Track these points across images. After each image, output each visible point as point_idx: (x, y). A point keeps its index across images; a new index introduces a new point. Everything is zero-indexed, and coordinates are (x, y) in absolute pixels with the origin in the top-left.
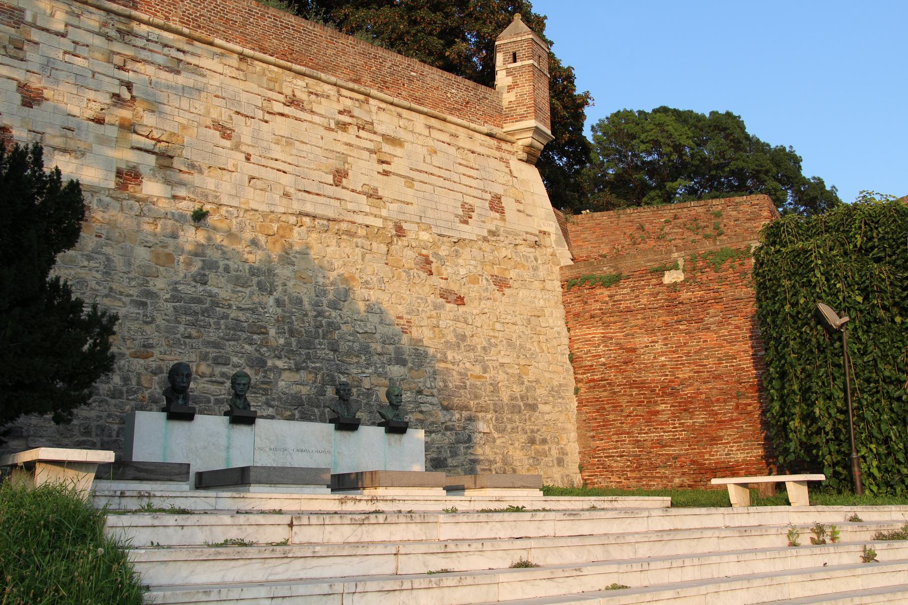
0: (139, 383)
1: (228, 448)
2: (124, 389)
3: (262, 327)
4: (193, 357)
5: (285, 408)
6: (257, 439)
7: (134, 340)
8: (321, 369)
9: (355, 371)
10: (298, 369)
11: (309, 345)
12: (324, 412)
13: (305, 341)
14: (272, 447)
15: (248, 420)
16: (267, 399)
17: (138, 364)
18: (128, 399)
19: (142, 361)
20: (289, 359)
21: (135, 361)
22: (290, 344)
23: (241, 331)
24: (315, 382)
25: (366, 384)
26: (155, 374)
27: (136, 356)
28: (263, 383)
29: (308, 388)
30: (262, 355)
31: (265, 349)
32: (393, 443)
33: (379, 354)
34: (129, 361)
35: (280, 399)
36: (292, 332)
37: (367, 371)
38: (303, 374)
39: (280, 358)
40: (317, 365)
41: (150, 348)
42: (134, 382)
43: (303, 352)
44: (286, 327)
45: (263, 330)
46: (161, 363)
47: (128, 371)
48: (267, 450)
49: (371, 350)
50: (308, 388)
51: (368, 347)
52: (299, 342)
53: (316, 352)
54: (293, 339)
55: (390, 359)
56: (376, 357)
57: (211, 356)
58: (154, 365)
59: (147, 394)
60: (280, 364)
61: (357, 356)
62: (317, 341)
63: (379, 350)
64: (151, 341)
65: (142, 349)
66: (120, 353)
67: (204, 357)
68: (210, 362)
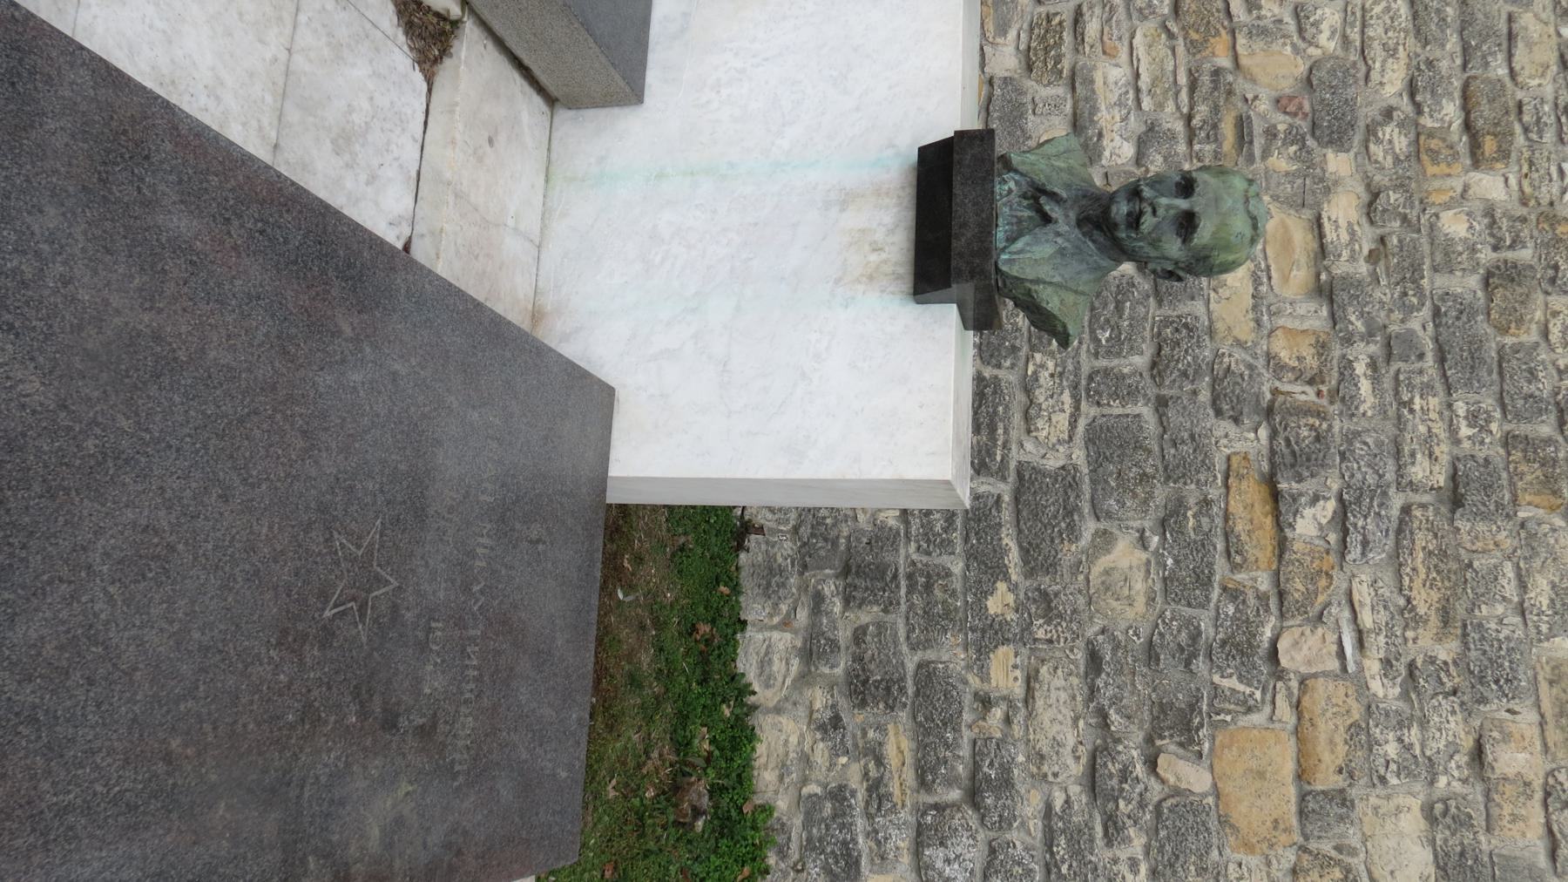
3: (1504, 137)
8: (1343, 395)
9: (1363, 593)
10: (1325, 291)
11: (1457, 359)
12: (1133, 394)
13: (1475, 347)
16: (1172, 137)
20: (1372, 257)
22: (1446, 265)
23: (1466, 50)
24: (1279, 368)
25: (1303, 650)
28: (1242, 125)
29: (1245, 331)
30: (1371, 131)
31: (1402, 143)
32: (854, 219)
33: (1478, 753)
36: (1498, 277)
37: (1373, 666)
38: (1314, 316)
39: (1370, 209)
40: (1365, 386)
43: (1419, 324)
44: (1525, 255)
45: (1489, 145)
49: (1496, 708)
50: (1245, 331)
51: (1508, 685)
52: (1465, 311)
53: (1427, 390)
54: (1474, 281)
55: (1463, 822)
56: (1450, 728)
60: (1343, 210)
61: (1446, 618)
62: (1488, 402)
63: (1511, 760)
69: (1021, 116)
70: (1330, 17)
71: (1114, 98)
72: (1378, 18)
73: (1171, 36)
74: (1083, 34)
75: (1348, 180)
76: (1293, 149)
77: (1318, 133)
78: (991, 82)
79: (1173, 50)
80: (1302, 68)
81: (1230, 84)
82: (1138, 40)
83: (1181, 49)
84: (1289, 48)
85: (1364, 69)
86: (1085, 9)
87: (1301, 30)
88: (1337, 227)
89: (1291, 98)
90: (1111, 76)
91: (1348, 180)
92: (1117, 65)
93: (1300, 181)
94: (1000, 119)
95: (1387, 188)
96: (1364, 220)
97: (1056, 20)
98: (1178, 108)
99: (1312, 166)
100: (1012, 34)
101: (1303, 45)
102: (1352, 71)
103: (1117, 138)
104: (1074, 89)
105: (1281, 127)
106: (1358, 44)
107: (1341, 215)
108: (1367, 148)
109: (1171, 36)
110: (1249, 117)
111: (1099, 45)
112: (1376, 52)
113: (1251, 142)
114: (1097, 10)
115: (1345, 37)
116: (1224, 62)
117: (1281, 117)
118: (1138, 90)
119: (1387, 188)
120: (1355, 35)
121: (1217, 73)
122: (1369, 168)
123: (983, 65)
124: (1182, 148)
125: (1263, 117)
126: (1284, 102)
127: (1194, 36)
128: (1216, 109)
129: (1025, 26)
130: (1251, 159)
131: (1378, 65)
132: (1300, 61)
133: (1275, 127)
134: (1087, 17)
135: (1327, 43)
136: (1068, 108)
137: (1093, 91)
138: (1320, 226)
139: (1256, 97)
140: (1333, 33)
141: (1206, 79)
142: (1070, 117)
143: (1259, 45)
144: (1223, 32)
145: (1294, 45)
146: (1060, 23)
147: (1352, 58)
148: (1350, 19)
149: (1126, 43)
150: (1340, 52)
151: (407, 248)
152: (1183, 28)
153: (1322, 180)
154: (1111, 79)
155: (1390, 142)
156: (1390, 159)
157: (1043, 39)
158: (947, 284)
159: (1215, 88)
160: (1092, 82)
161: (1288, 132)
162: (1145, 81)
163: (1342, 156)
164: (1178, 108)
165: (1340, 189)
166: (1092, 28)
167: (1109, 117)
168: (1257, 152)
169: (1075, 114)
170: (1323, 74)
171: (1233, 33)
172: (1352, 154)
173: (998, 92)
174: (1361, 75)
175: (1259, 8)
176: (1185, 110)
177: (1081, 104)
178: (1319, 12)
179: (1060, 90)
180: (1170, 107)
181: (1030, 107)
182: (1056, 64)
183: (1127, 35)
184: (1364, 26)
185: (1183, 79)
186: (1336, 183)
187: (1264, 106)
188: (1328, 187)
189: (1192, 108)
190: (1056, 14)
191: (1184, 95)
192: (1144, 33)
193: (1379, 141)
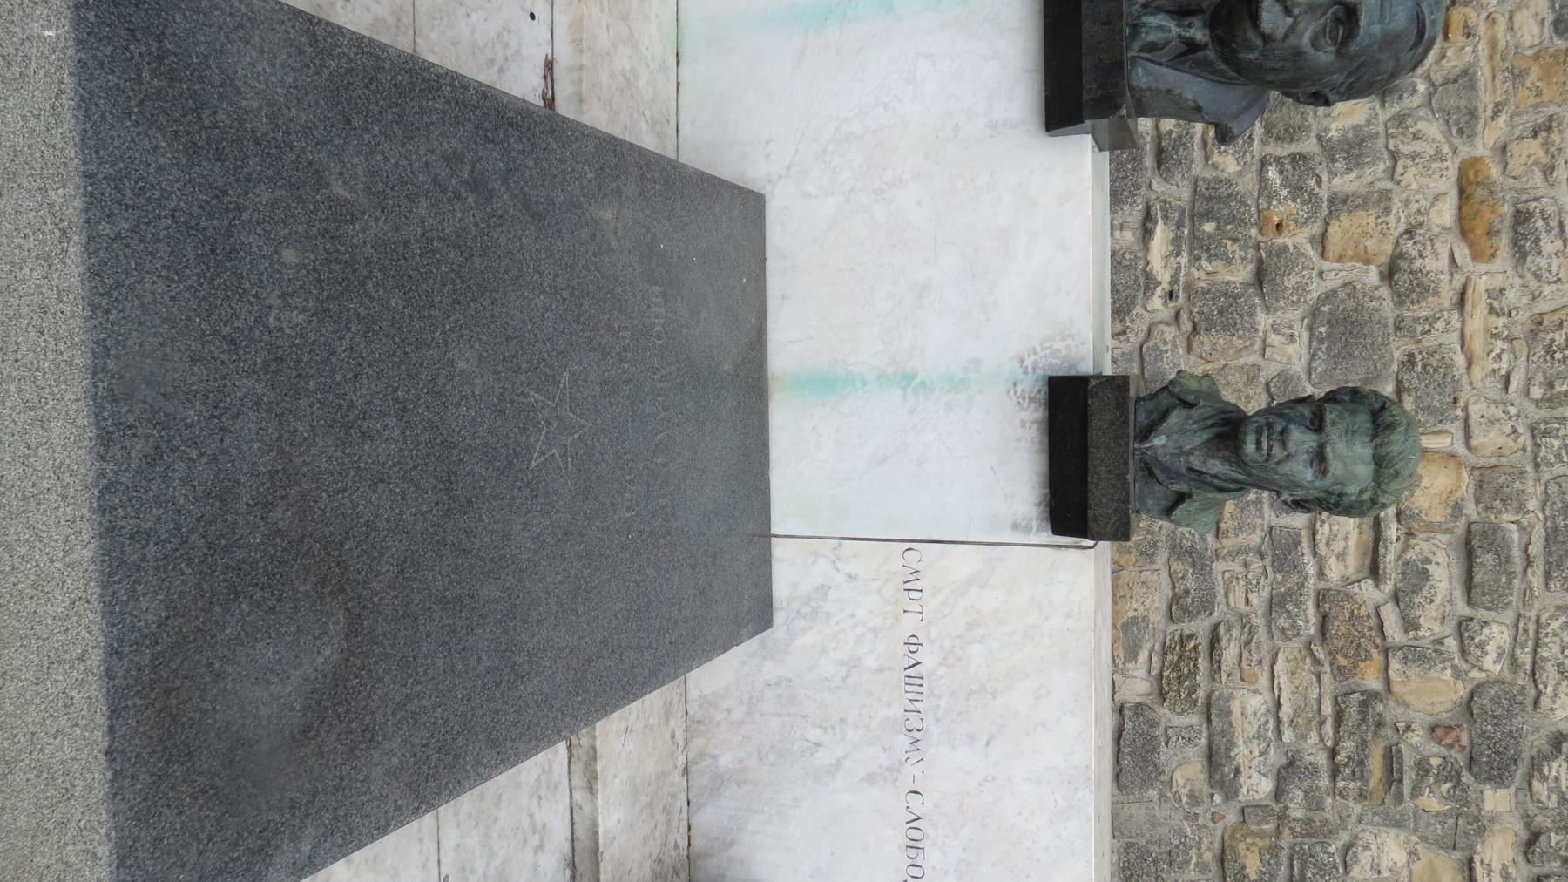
0: (1340, 203)
1: (906, 380)
2: (1309, 146)
4: (1489, 440)
5: (1274, 850)
6: (965, 562)
7: (1548, 171)
14: (928, 659)
15: (1074, 502)
16: (1314, 771)
17: (1431, 192)
18: (1264, 163)
19: (1445, 213)
21: (1446, 184)
26: (1390, 273)
27: (1468, 185)
28: (1392, 758)
30: (1535, 766)
34: (1438, 156)
35: (1324, 833)
39: (1530, 843)
41: (1515, 243)
42: (1346, 182)
46: (1447, 295)
47: (1394, 156)
48: (909, 625)
57: (1507, 518)
58: (1435, 264)
59: (1298, 239)
64: (1550, 245)
65: (1507, 209)
66: (1473, 114)
67: (1492, 485)
68: (1471, 510)
69: (1154, 750)
70: (1498, 851)
71: (1253, 731)
72: (1555, 635)
73: (1316, 661)
74: (1219, 662)
75: (1507, 817)
76: (1446, 787)
77: (1475, 769)
78: (1120, 710)
79: (1318, 676)
80: (1462, 691)
81: (1380, 715)
82: (1279, 667)
83: (1327, 678)
84: (1449, 672)
85: (1532, 692)
86: (1222, 631)
87: (1464, 653)
88: (1490, 871)
89: (1450, 728)
90: (1249, 706)
91: (1507, 817)
92: (1256, 692)
93: (1451, 821)
94: (1131, 754)
95: (1549, 830)
96: (1520, 859)
97: (1192, 644)
98: (1322, 739)
99: (1467, 803)
100: (1143, 656)
101: (1465, 667)
102: (1519, 698)
103: (1255, 775)
104: (1209, 721)
105: (1435, 762)
106: (1528, 667)
107: (1495, 857)
108: (1530, 785)
109: (1316, 661)
110: (1399, 751)
111: (1237, 673)
112: (1550, 674)
113: (1400, 781)
114: (1235, 633)
115: (1514, 663)
116: (1373, 683)
117: (1435, 748)
118: (1279, 721)
119: (1549, 830)
120: (1525, 657)
121: (1370, 698)
122: (1530, 806)
123: (1114, 693)
124: (1324, 782)
125: (1415, 748)
126: (1439, 732)
127: (1342, 661)
128: (1363, 745)
129: (1158, 647)
130: (1399, 798)
131: (1550, 688)
132: (1460, 685)
133: (1427, 759)
134: (1224, 643)
135: (1492, 665)
136: (1204, 741)
137: (1231, 725)
138: (1471, 870)
139: (1408, 728)
140: (1500, 655)
141: (1353, 711)
142: (1205, 749)
143: (1414, 671)
144: (1374, 652)
145: (1455, 668)
146: (1195, 648)
147: (1520, 682)
148: (1521, 638)
149: (1266, 667)
150: (1507, 675)
151: (550, 103)
152: (1330, 653)
153: (1476, 819)
154: (1249, 710)
155: (1557, 779)
156: (1554, 798)
157: (1176, 667)
158: (1080, 120)
159: (1363, 720)
160: (1229, 713)
161: (1441, 768)
162: (1286, 712)
163: (1502, 792)
164: (1322, 739)
165: (1497, 827)
166: (1230, 653)
167: (1247, 753)
168: (1407, 789)
169: (1210, 747)
170: (1486, 702)
171: (1386, 651)
172: (1512, 789)
173: (1128, 725)
174: (1529, 702)
175: (1417, 627)
176: (1329, 744)
177: (1217, 738)
178: (1486, 631)
179: (1194, 719)
180: (1313, 737)
181: (1163, 739)
182: (1190, 694)
183: (1267, 658)
184: (1537, 645)
185: (1328, 709)
186: (1492, 820)
187: (1416, 738)
188: (1481, 826)
189: (1336, 743)
190: (1191, 636)
191: (1328, 728)
192: (1290, 650)
193: (1544, 778)
